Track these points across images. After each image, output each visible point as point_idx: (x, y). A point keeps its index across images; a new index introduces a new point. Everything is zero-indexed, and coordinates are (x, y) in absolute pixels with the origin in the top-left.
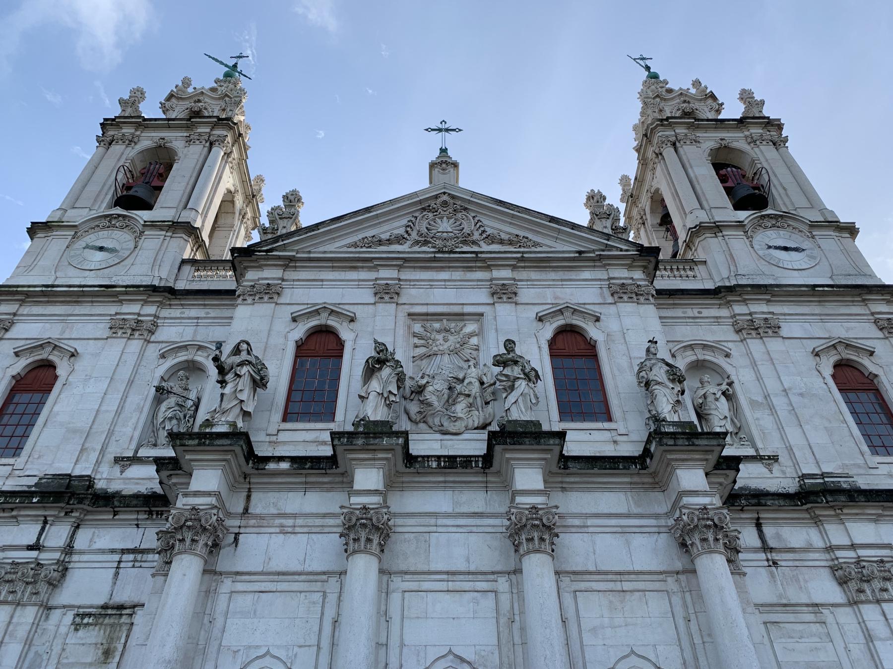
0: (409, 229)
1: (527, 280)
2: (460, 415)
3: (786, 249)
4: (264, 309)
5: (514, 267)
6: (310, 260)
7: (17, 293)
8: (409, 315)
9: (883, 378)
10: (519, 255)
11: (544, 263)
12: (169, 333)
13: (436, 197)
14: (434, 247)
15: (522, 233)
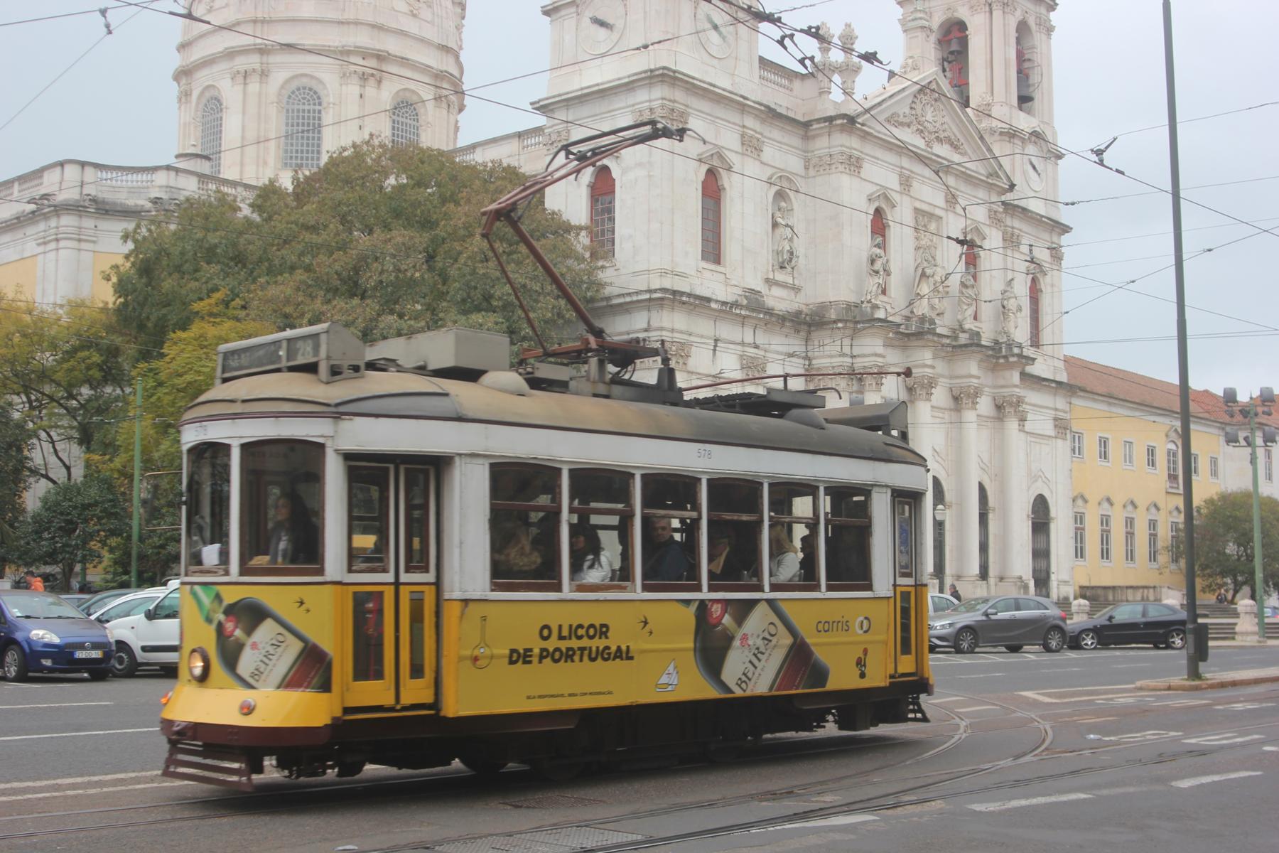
0: (913, 112)
1: (961, 192)
2: (937, 307)
3: (1034, 168)
4: (856, 181)
5: (957, 175)
6: (876, 137)
7: (687, 82)
8: (916, 209)
9: (1044, 295)
10: (963, 170)
11: (967, 178)
12: (769, 153)
13: (930, 82)
14: (924, 138)
15: (962, 140)
